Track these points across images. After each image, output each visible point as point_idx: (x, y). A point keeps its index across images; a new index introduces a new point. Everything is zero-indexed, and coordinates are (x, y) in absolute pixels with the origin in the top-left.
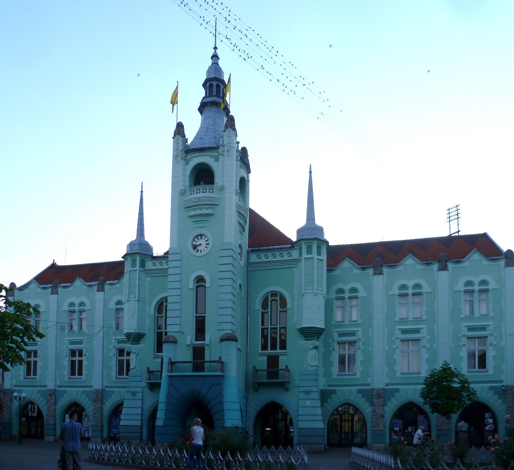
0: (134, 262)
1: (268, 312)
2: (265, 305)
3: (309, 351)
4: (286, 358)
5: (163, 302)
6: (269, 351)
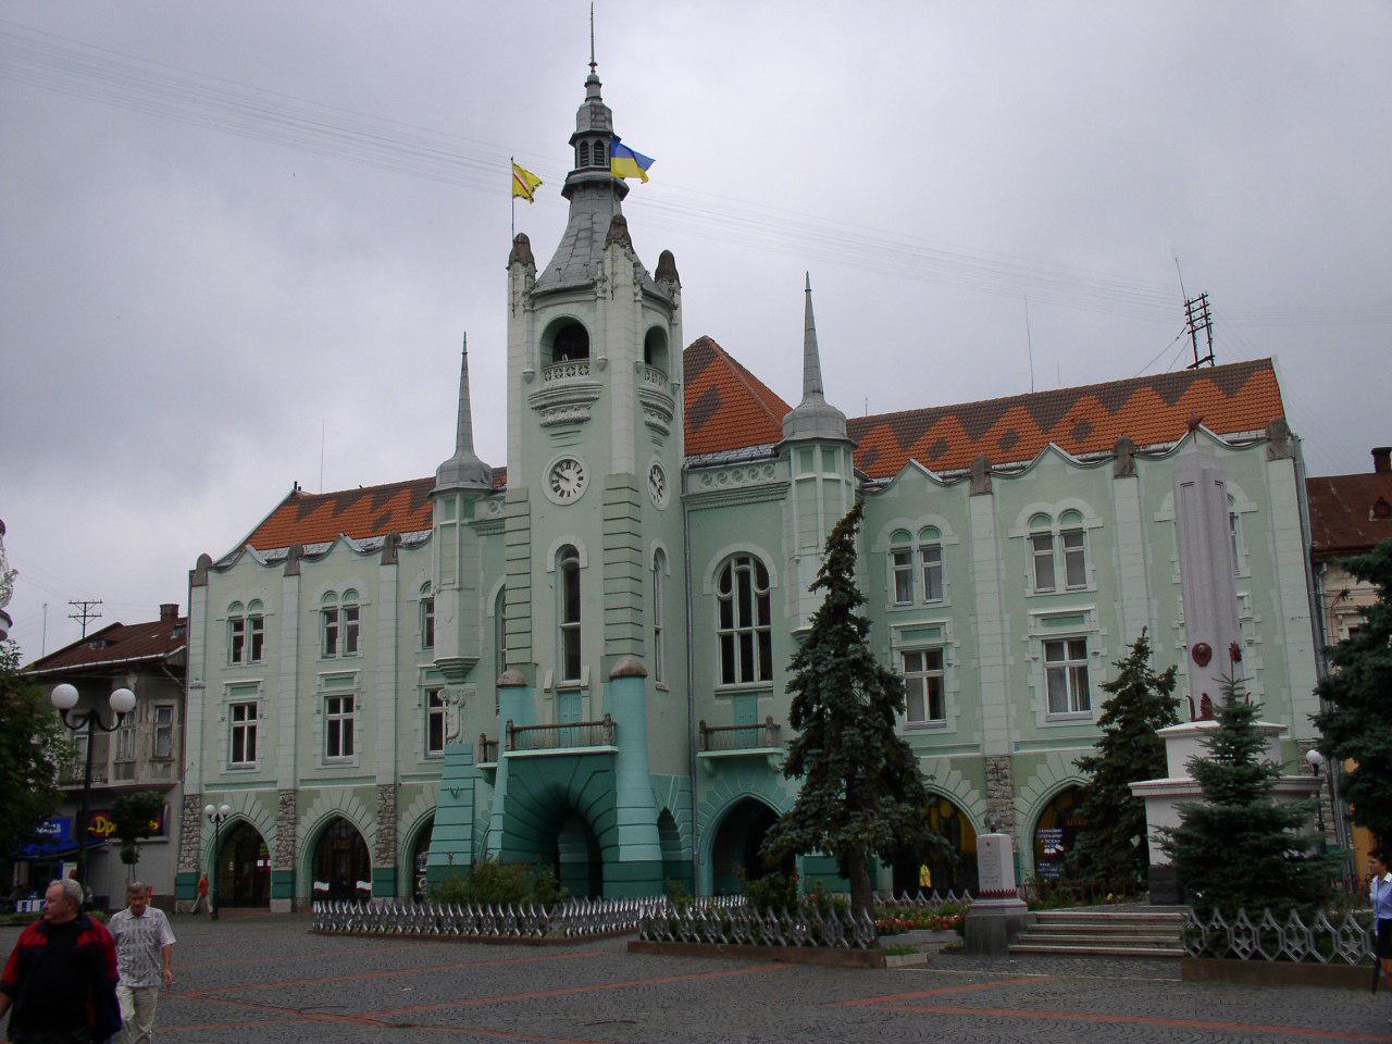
0: (450, 502)
2: (725, 585)
4: (770, 698)
6: (738, 683)
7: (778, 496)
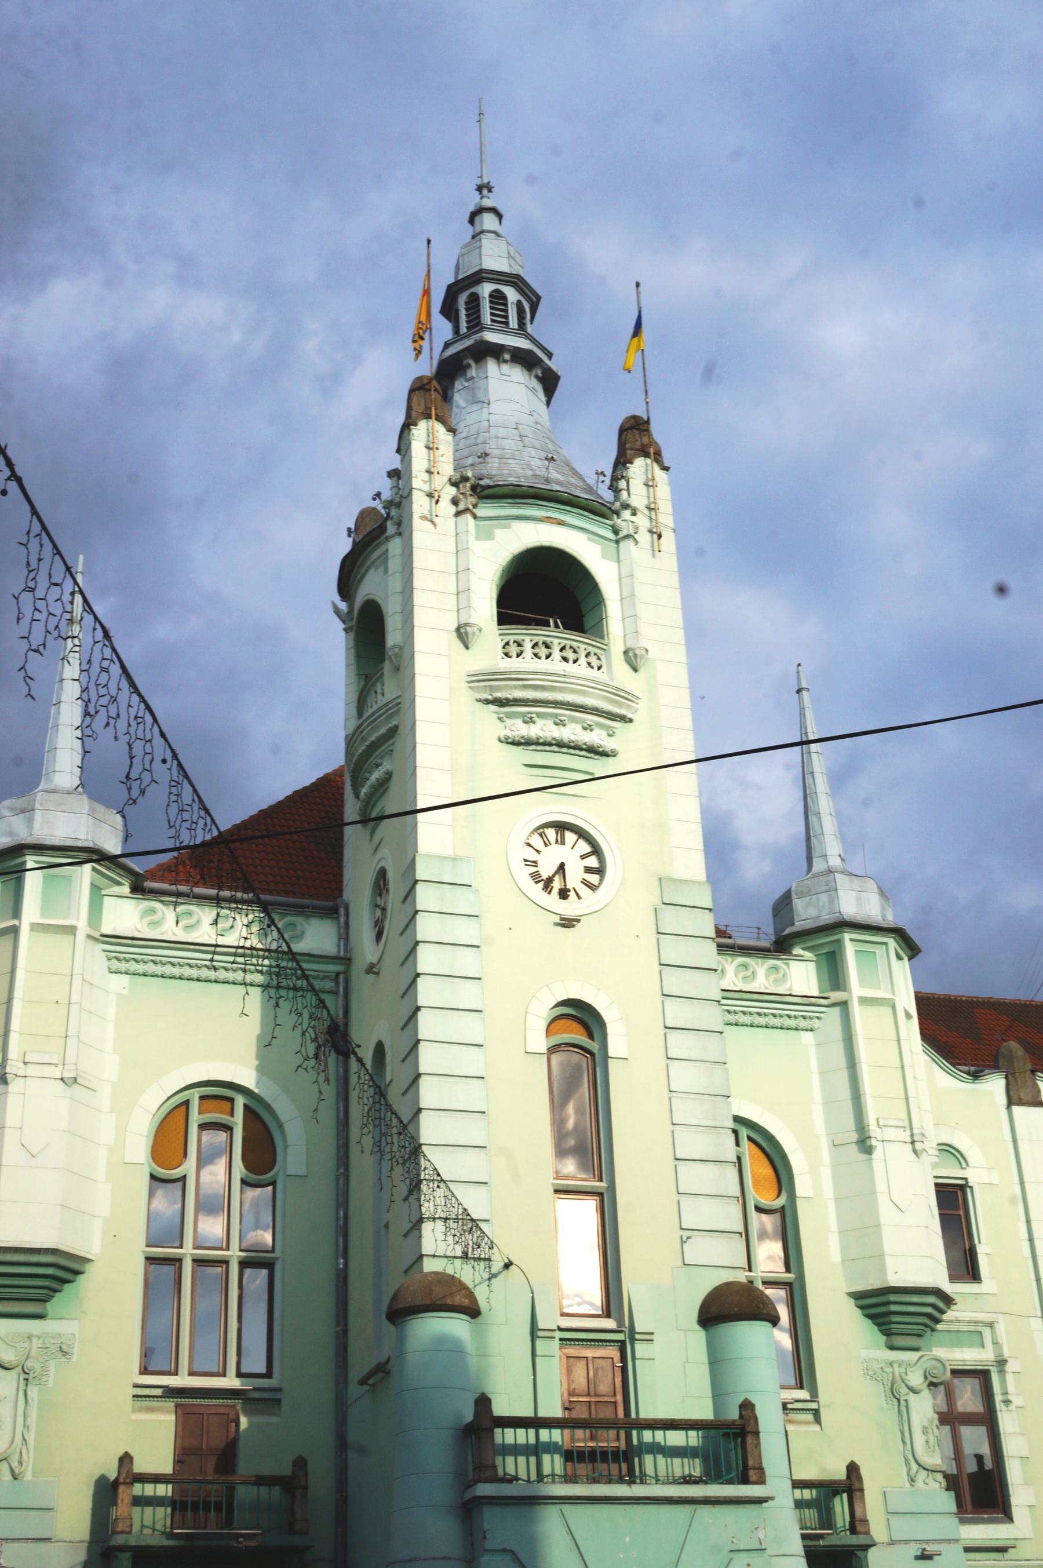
3: (912, 1397)
4: (817, 1428)
5: (187, 1103)
7: (802, 1023)
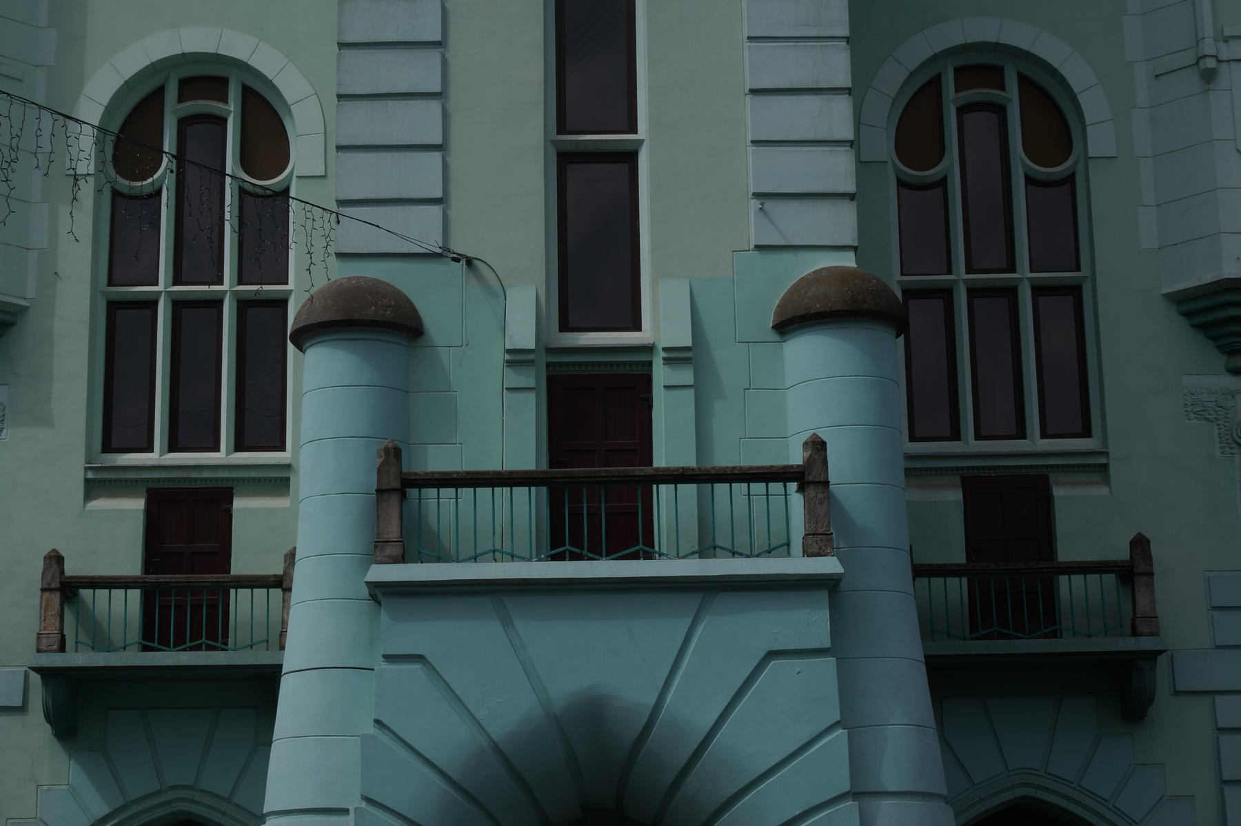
1: (943, 183)
4: (1103, 491)
